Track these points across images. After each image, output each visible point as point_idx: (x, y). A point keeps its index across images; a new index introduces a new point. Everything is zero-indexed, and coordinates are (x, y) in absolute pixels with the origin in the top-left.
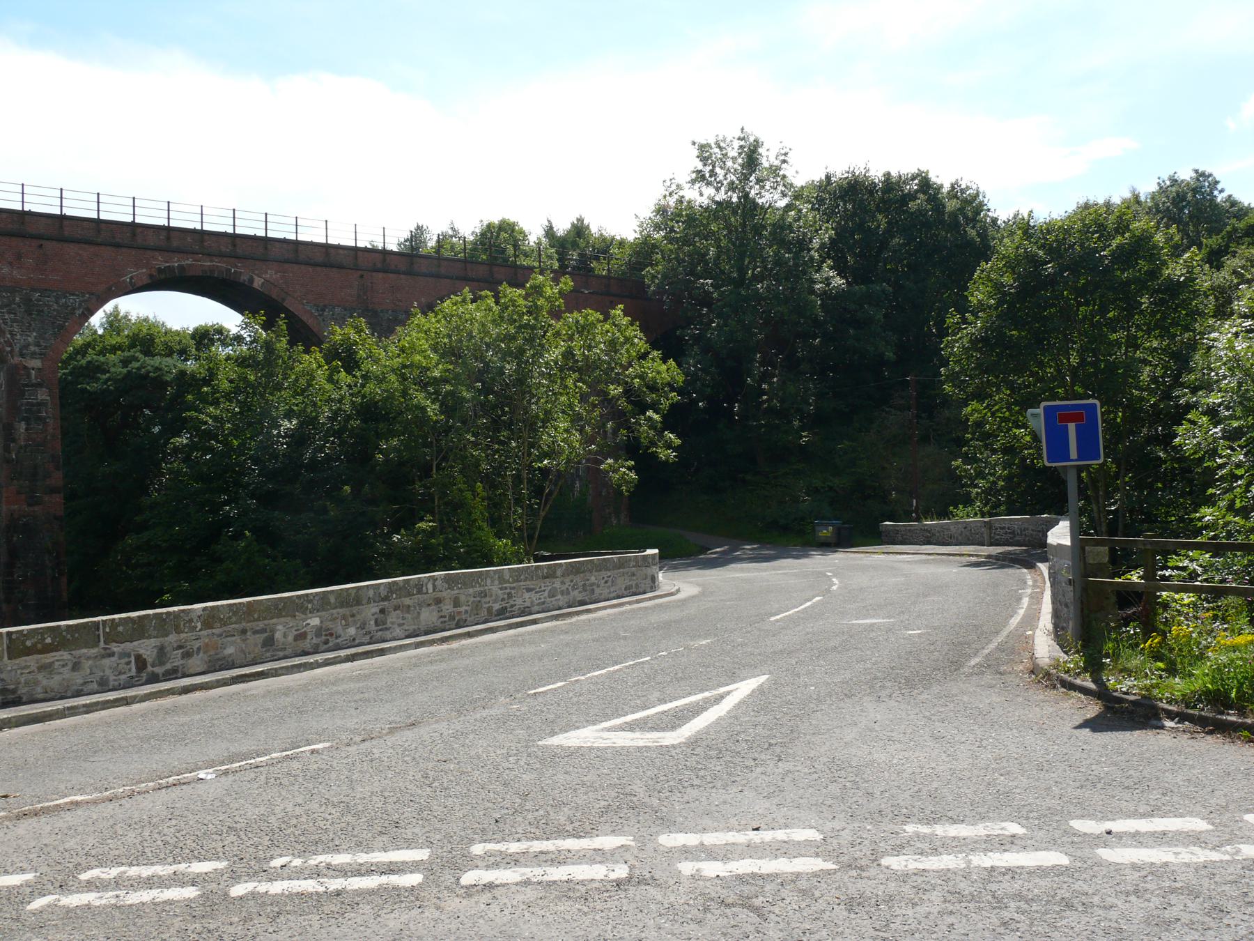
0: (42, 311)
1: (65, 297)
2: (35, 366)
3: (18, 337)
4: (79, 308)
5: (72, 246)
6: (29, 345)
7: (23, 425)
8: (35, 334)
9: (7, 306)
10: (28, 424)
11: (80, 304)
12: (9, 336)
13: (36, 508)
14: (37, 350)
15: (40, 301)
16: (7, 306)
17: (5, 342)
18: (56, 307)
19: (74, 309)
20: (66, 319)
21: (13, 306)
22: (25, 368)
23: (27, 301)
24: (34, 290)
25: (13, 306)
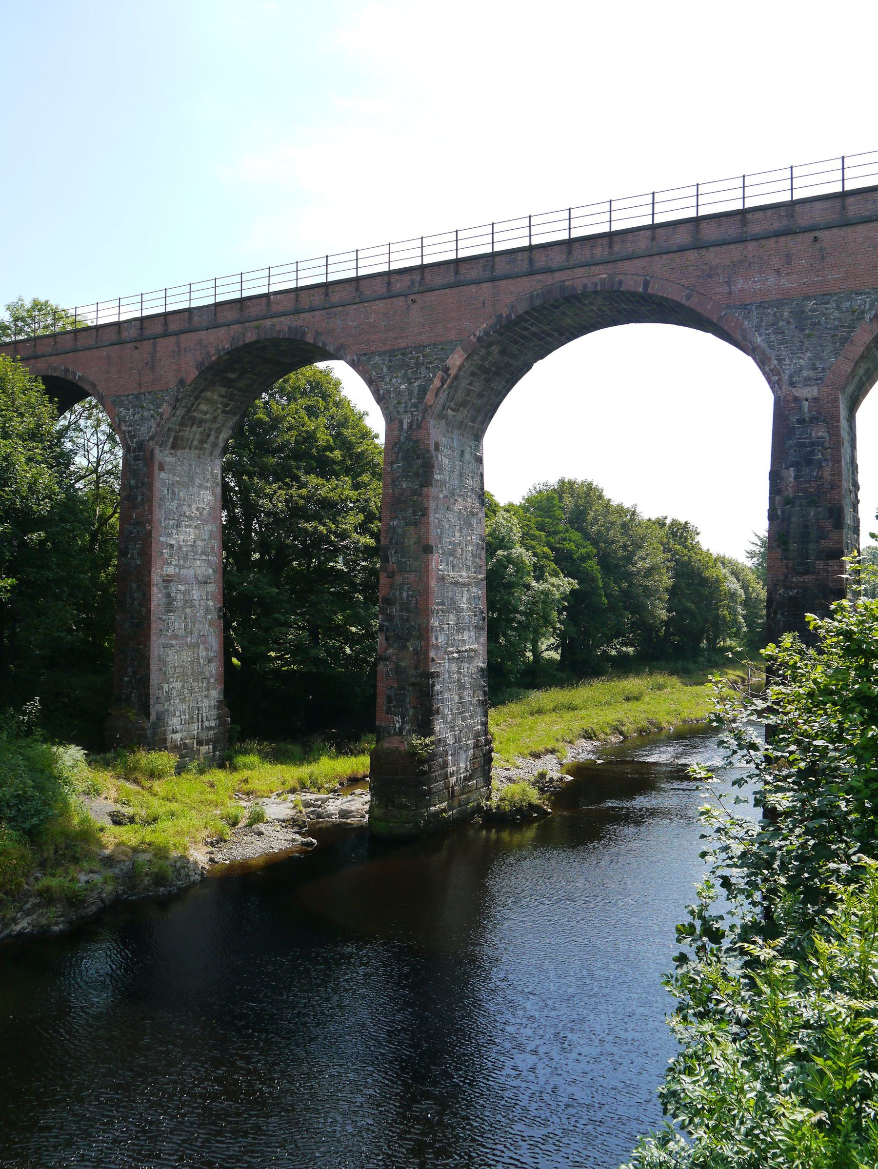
0: (819, 323)
1: (850, 299)
2: (809, 396)
3: (787, 362)
4: (870, 309)
5: (859, 228)
6: (801, 369)
7: (792, 472)
8: (809, 354)
9: (773, 325)
10: (798, 471)
11: (872, 305)
12: (776, 362)
13: (807, 578)
14: (811, 373)
15: (816, 310)
16: (773, 325)
17: (771, 370)
18: (837, 314)
19: (863, 312)
20: (852, 328)
21: (781, 323)
22: (796, 399)
23: (799, 315)
24: (808, 298)
25: (781, 323)
